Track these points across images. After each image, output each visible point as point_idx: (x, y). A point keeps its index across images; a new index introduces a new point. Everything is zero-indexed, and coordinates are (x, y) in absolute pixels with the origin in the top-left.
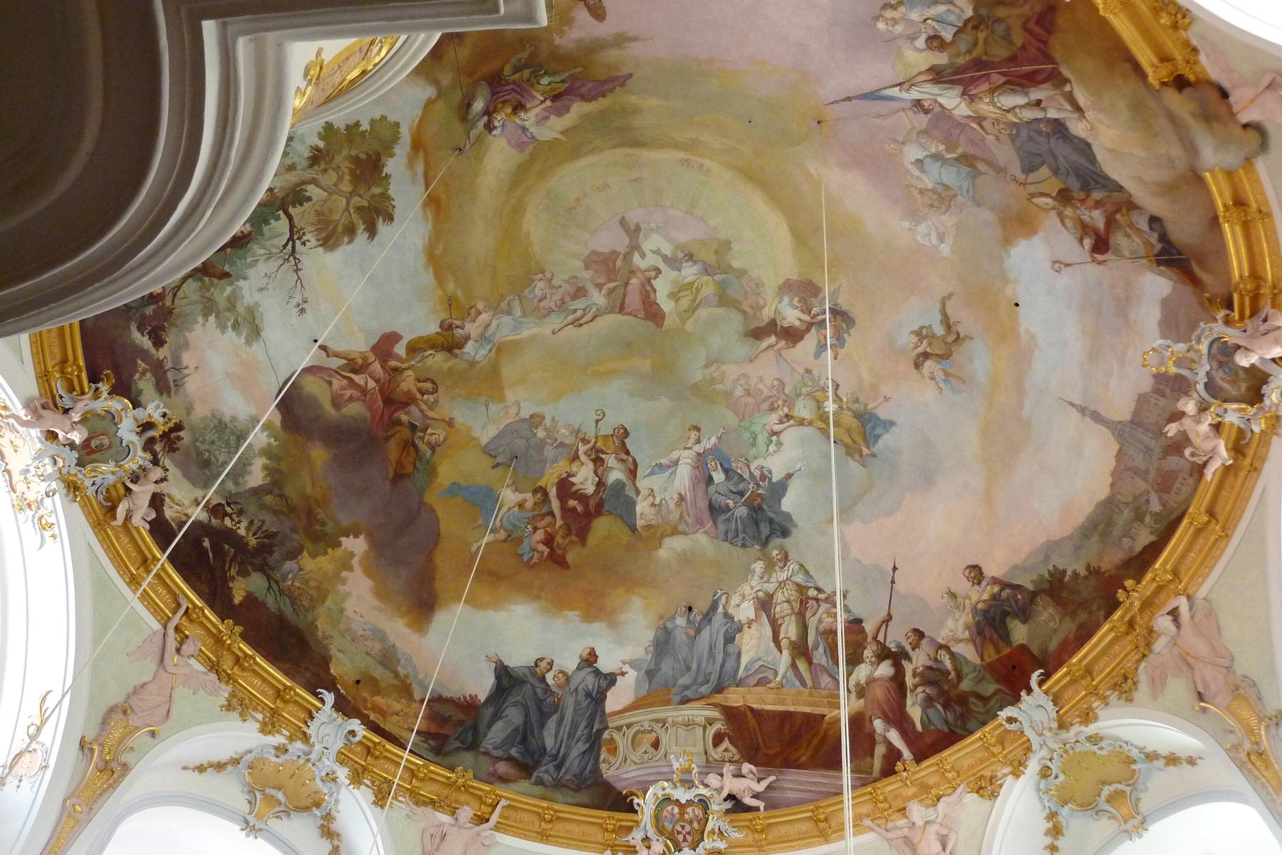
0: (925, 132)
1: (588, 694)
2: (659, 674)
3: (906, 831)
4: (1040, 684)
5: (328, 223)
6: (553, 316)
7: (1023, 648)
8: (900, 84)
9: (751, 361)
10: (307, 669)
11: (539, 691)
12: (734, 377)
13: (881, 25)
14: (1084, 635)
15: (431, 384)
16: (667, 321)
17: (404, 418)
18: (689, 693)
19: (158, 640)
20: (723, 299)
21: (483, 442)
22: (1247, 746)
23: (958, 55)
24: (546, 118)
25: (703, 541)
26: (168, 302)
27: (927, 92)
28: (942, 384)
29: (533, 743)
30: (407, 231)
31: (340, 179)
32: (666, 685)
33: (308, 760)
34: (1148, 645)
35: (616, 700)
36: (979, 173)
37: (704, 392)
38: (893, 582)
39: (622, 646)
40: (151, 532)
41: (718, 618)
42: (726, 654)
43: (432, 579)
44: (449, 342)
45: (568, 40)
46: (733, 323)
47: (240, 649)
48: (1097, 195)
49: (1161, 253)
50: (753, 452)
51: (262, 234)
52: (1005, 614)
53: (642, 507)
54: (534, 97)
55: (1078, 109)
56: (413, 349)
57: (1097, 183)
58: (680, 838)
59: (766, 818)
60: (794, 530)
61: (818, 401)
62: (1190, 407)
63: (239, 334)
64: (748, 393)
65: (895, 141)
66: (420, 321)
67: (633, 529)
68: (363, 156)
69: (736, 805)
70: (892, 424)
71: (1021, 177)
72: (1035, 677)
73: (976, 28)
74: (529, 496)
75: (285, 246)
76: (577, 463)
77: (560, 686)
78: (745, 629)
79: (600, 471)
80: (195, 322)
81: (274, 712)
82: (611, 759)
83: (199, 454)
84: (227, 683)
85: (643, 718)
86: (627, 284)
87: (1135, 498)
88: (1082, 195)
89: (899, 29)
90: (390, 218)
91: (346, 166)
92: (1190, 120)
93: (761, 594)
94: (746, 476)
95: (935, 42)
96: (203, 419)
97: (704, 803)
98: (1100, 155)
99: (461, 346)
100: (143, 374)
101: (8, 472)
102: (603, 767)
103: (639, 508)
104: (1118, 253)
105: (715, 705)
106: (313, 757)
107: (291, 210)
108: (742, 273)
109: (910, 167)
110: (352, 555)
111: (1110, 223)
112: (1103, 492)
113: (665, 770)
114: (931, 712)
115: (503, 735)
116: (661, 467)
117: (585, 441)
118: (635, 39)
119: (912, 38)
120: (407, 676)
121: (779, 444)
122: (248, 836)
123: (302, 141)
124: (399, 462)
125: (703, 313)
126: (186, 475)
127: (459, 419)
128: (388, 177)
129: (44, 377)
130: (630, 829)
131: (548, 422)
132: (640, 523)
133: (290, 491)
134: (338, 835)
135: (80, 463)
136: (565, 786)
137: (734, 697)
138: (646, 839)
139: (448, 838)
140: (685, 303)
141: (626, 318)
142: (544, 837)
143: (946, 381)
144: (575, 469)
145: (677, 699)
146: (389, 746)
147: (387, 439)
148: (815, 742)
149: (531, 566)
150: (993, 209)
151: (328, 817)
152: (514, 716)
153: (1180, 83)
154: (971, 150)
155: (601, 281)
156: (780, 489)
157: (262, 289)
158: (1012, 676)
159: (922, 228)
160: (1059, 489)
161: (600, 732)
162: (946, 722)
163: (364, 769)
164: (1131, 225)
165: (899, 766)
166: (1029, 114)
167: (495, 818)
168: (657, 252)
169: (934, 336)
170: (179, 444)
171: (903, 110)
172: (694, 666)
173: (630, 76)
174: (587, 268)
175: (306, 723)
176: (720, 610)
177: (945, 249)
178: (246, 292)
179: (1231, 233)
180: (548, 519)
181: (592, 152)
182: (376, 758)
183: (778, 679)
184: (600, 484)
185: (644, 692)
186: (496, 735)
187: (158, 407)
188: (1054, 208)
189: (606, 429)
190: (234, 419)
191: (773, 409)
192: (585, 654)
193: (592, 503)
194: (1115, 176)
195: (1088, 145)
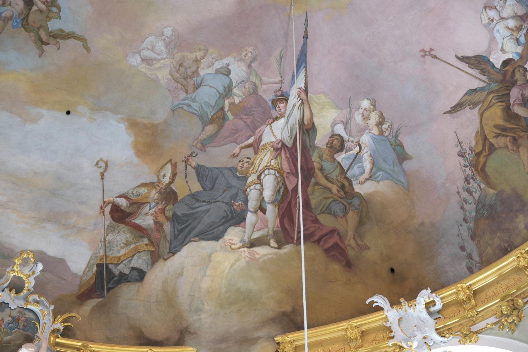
0: (255, 91)
8: (306, 91)
13: (366, 104)
23: (320, 157)
48: (167, 227)
55: (252, 244)
65: (253, 60)
71: (194, 162)
73: (342, 187)
88: (169, 213)
89: (358, 118)
95: (337, 144)
104: (110, 229)
109: (225, 61)
111: (140, 231)
119: (346, 124)
150: (166, 122)
154: (228, 126)
159: (160, 46)
164: (137, 251)
166: (253, 195)
171: (281, 82)
177: (135, 60)
188: (159, 181)
194: (186, 250)
195: (217, 238)
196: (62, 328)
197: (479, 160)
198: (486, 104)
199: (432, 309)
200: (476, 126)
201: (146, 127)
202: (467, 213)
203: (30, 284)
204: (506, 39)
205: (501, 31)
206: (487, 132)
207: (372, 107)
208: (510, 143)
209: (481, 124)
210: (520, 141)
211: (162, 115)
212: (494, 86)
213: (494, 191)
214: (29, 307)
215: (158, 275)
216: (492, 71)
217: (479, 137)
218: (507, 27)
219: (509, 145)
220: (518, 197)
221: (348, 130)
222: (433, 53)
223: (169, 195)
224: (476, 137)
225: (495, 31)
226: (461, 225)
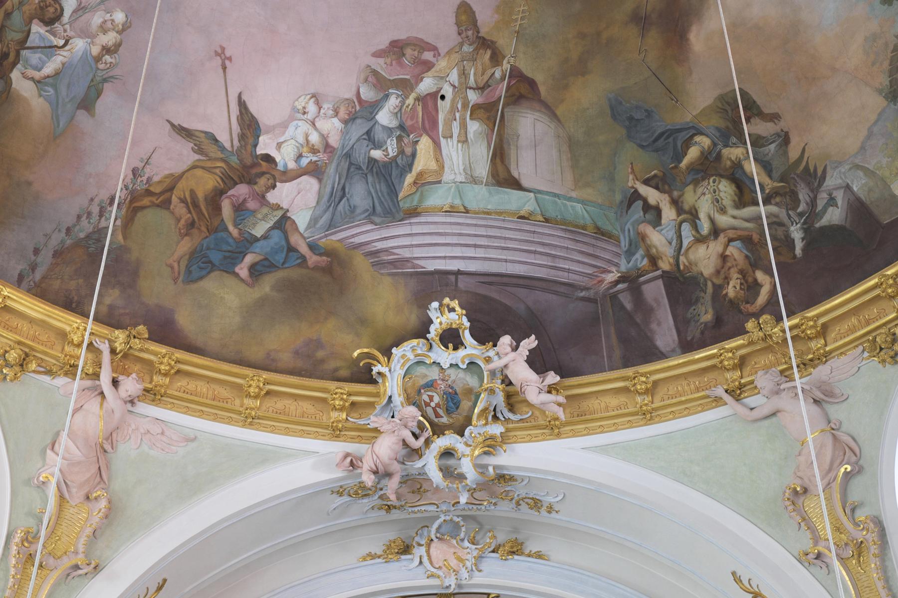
13: (119, 17)
89: (97, 19)
197: (144, 198)
198: (209, 164)
200: (177, 168)
202: (77, 227)
204: (293, 142)
205: (298, 131)
206: (180, 185)
207: (120, 27)
208: (186, 221)
209: (184, 173)
210: (195, 231)
212: (234, 161)
213: (122, 241)
216: (249, 147)
217: (168, 181)
218: (307, 136)
219: (182, 222)
221: (76, 16)
222: (227, 62)
224: (167, 177)
225: (295, 122)
226: (59, 230)
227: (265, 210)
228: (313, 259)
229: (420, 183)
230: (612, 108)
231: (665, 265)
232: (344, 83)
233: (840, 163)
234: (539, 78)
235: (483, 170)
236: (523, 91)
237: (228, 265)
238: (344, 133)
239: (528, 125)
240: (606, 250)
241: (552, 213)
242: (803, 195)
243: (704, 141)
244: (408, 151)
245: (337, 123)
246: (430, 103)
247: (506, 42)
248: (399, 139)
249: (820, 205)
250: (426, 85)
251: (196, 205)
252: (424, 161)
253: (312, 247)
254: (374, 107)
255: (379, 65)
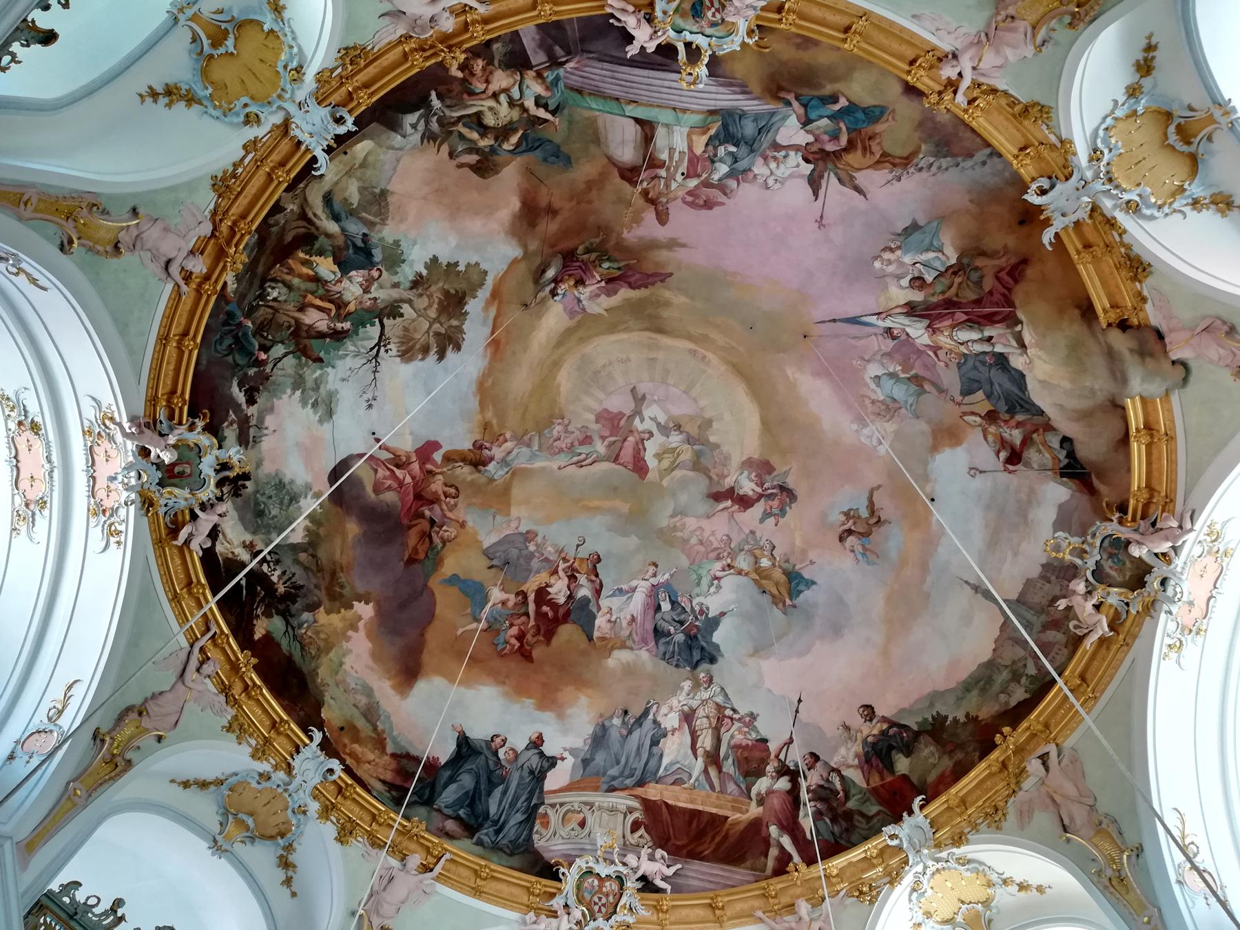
0: (889, 355)
1: (532, 772)
2: (592, 764)
3: (793, 925)
4: (922, 807)
5: (413, 339)
6: (563, 455)
7: (905, 777)
8: (879, 314)
9: (708, 517)
10: (301, 709)
11: (491, 762)
12: (692, 528)
13: (877, 264)
14: (959, 772)
15: (454, 489)
16: (650, 476)
17: (427, 513)
18: (615, 783)
19: (183, 656)
20: (697, 466)
21: (486, 545)
22: (1109, 873)
23: (933, 295)
24: (598, 296)
25: (644, 657)
26: (268, 370)
27: (899, 322)
28: (860, 557)
29: (480, 808)
30: (467, 363)
31: (430, 306)
32: (597, 774)
33: (286, 790)
34: (1018, 783)
35: (555, 780)
36: (925, 392)
37: (668, 537)
38: (797, 711)
39: (566, 734)
40: (201, 559)
41: (648, 723)
42: (651, 754)
43: (421, 652)
44: (477, 460)
45: (632, 235)
46: (700, 485)
47: (251, 679)
48: (1020, 417)
49: (1066, 467)
50: (697, 590)
51: (357, 334)
52: (891, 748)
53: (601, 621)
54: (594, 277)
55: (1023, 346)
56: (448, 458)
57: (1022, 406)
58: (596, 908)
59: (672, 900)
60: (720, 659)
61: (756, 558)
62: (1080, 587)
63: (315, 413)
64: (701, 543)
65: (863, 359)
66: (458, 436)
67: (590, 639)
68: (453, 292)
69: (647, 885)
70: (814, 583)
71: (959, 398)
72: (917, 801)
73: (955, 273)
74: (512, 597)
75: (372, 349)
76: (555, 576)
77: (508, 761)
78: (669, 735)
79: (572, 586)
80: (285, 392)
81: (267, 741)
82: (544, 832)
83: (257, 503)
84: (232, 707)
85: (575, 799)
86: (625, 440)
87: (1014, 662)
88: (1007, 417)
89: (891, 269)
90: (458, 347)
91: (438, 296)
92: (1126, 354)
93: (686, 708)
94: (688, 609)
95: (918, 282)
96: (267, 476)
97: (620, 879)
98: (1031, 385)
99: (485, 465)
100: (231, 424)
101: (94, 478)
102: (535, 837)
103: (597, 622)
104: (1028, 465)
105: (636, 797)
106: (291, 788)
107: (385, 321)
108: (717, 446)
109: (869, 381)
110: (360, 618)
111: (1027, 441)
112: (986, 655)
113: (588, 847)
114: (820, 824)
115: (455, 797)
116: (621, 591)
117: (565, 560)
118: (683, 246)
119: (899, 277)
120: (384, 732)
121: (719, 587)
122: (213, 854)
123: (411, 267)
124: (415, 550)
125: (678, 473)
126: (242, 519)
127: (470, 524)
128: (466, 313)
129: (152, 401)
130: (553, 895)
131: (539, 539)
132: (596, 634)
133: (322, 553)
134: (295, 866)
135: (161, 484)
136: (501, 850)
137: (653, 792)
138: (566, 906)
139: (395, 880)
140: (666, 463)
141: (618, 467)
142: (477, 892)
143: (863, 554)
144: (552, 581)
145: (605, 787)
146: (358, 789)
147: (410, 527)
148: (717, 839)
149: (501, 655)
150: (928, 422)
151: (289, 848)
152: (466, 781)
153: (1123, 325)
154: (922, 373)
155: (606, 433)
156: (714, 623)
157: (344, 380)
158: (895, 802)
159: (866, 431)
160: (950, 648)
161: (537, 806)
162: (833, 833)
163: (334, 806)
164: (1045, 443)
165: (791, 867)
166: (978, 348)
167: (438, 869)
168: (654, 419)
169: (859, 517)
170: (243, 492)
172: (623, 761)
173: (671, 274)
174: (597, 422)
175: (292, 757)
176: (651, 717)
178: (330, 378)
179: (1137, 450)
180: (524, 618)
181: (626, 330)
182: (345, 798)
183: (692, 781)
184: (570, 597)
185: (578, 777)
186: (449, 795)
187: (238, 452)
189: (584, 553)
190: (292, 482)
191: (718, 558)
192: (534, 737)
193: (561, 612)
195: (1023, 376)
196: (1117, 515)
199: (1046, 186)
201: (935, 438)
203: (1076, 541)
205: (783, 171)
206: (872, 162)
210: (870, 133)
211: (923, 426)
212: (830, 166)
214: (1098, 544)
215: (1066, 427)
220: (920, 125)
223: (991, 417)
227: (817, 132)
228: (791, 97)
229: (704, 129)
230: (570, 163)
231: (531, 73)
232: (746, 193)
233: (412, 148)
234: (618, 180)
235: (660, 132)
236: (630, 174)
237: (852, 108)
238: (753, 164)
239: (627, 154)
240: (575, 81)
241: (614, 103)
242: (435, 126)
243: (506, 146)
244: (710, 148)
245: (756, 170)
246: (691, 173)
247: (638, 201)
248: (715, 155)
249: (422, 122)
250: (692, 183)
251: (864, 149)
252: (700, 143)
253: (789, 104)
254: (729, 175)
255: (722, 198)
